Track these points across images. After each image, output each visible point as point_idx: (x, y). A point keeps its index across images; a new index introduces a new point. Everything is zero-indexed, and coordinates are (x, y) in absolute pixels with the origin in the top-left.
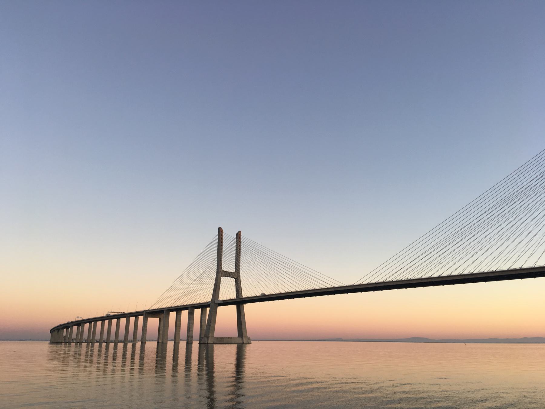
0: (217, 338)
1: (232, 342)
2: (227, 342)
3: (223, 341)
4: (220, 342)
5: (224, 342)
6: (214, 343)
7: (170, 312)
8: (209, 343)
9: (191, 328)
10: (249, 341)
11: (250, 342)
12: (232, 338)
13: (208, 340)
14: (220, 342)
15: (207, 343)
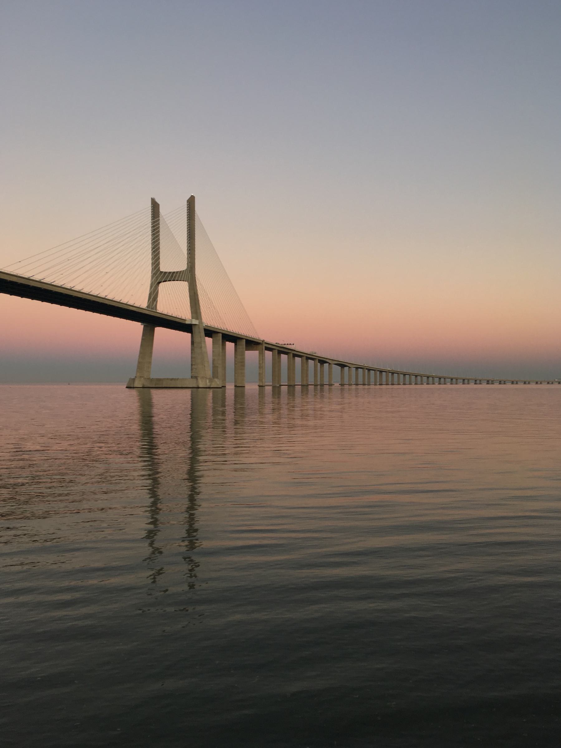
0: (152, 380)
1: (178, 386)
2: (168, 386)
3: (160, 385)
4: (155, 385)
5: (163, 386)
6: (146, 386)
7: (227, 341)
8: (134, 387)
9: (194, 365)
10: (211, 384)
11: (212, 386)
12: (178, 379)
13: (134, 384)
14: (156, 386)
15: (132, 386)
